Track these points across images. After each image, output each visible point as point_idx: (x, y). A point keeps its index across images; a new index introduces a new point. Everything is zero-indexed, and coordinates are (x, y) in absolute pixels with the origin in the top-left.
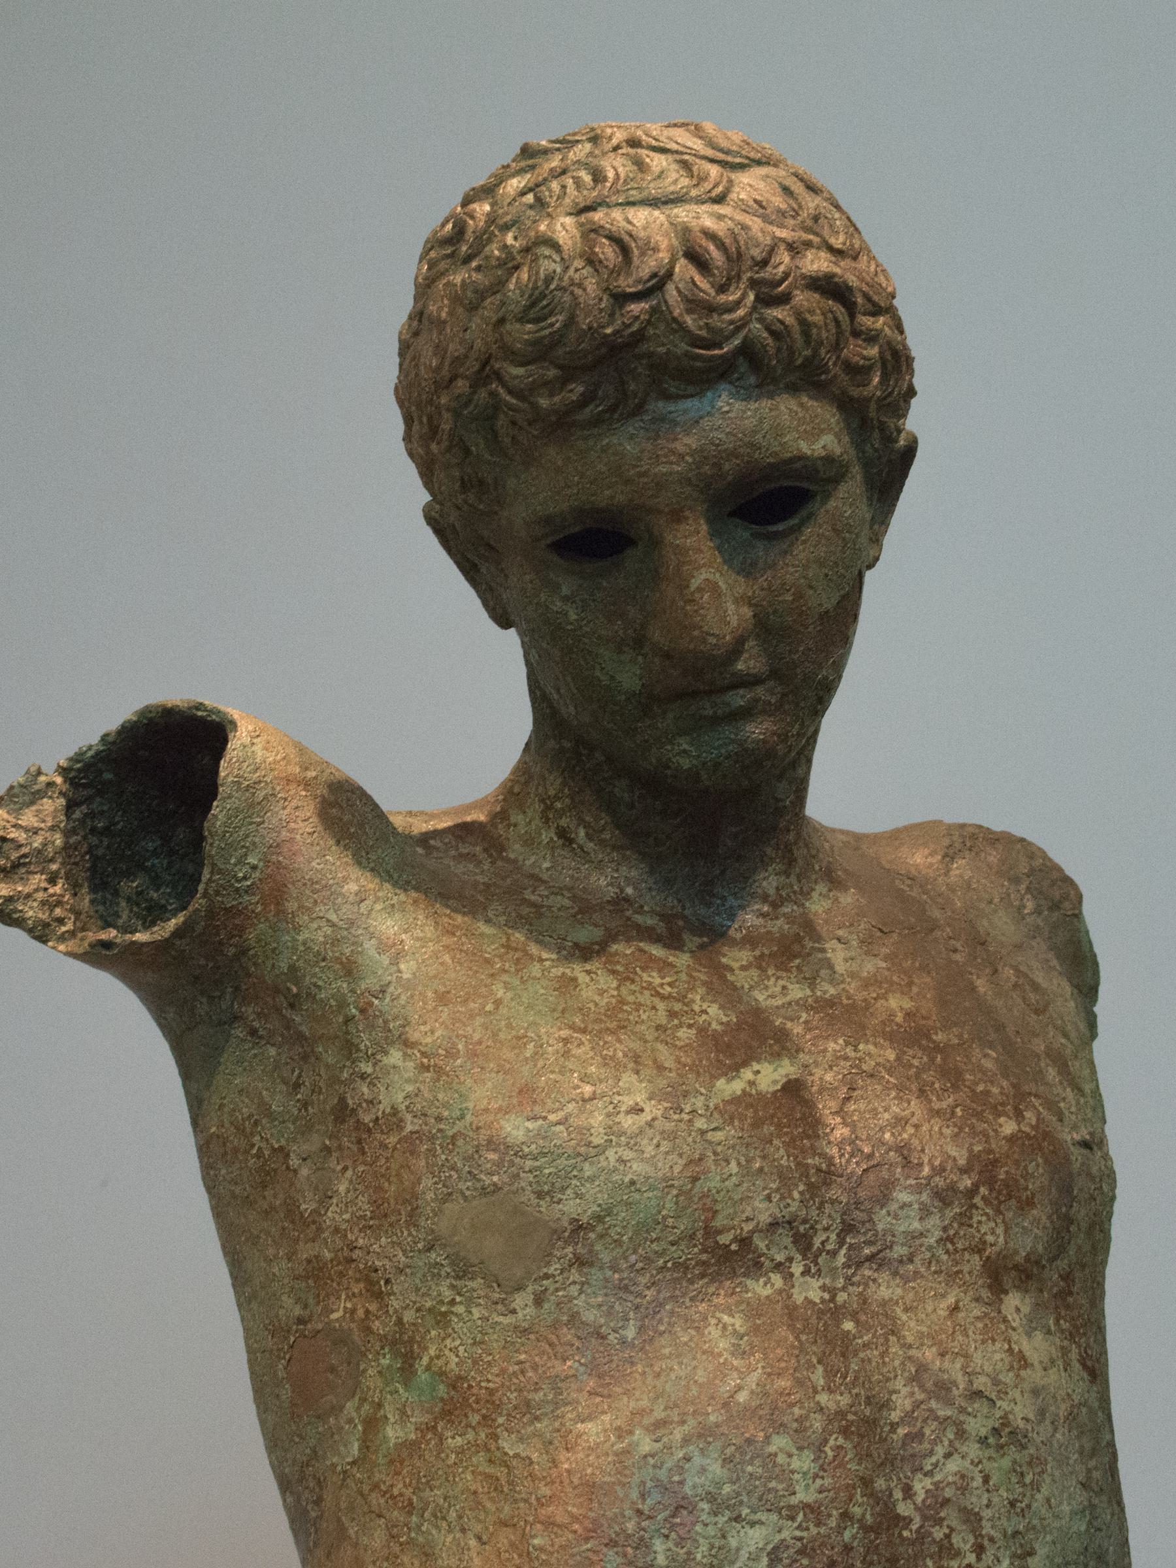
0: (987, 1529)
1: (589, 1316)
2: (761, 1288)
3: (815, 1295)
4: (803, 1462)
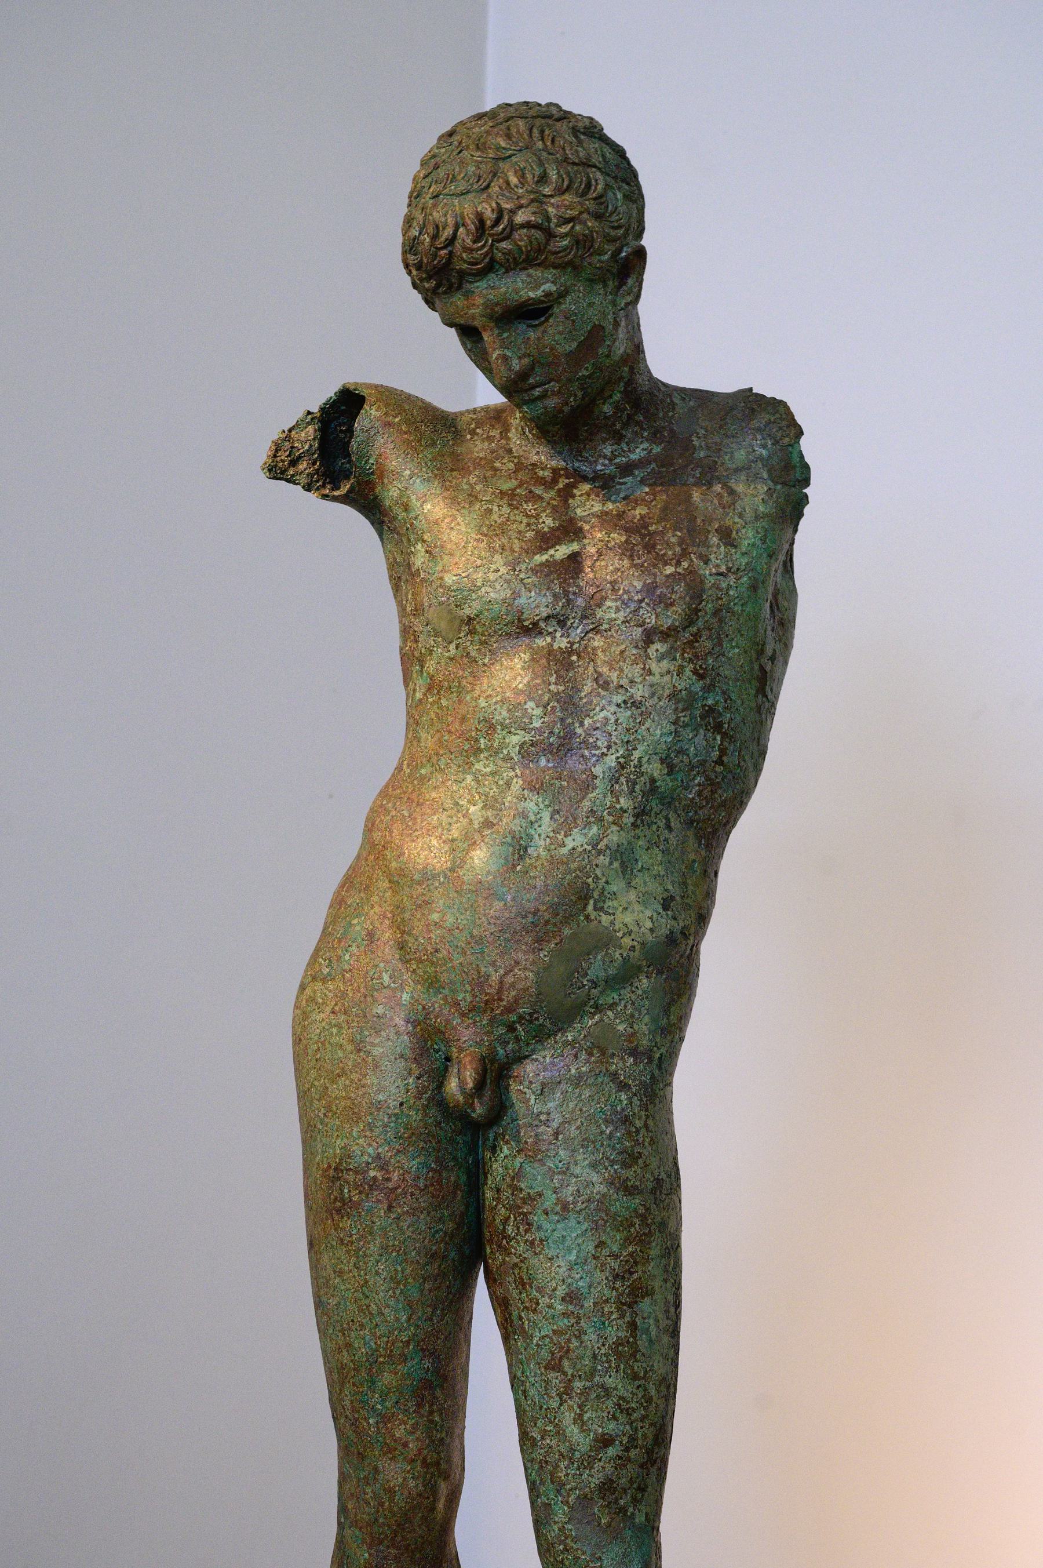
0: (614, 739)
1: (473, 654)
2: (540, 642)
3: (563, 646)
4: (538, 712)
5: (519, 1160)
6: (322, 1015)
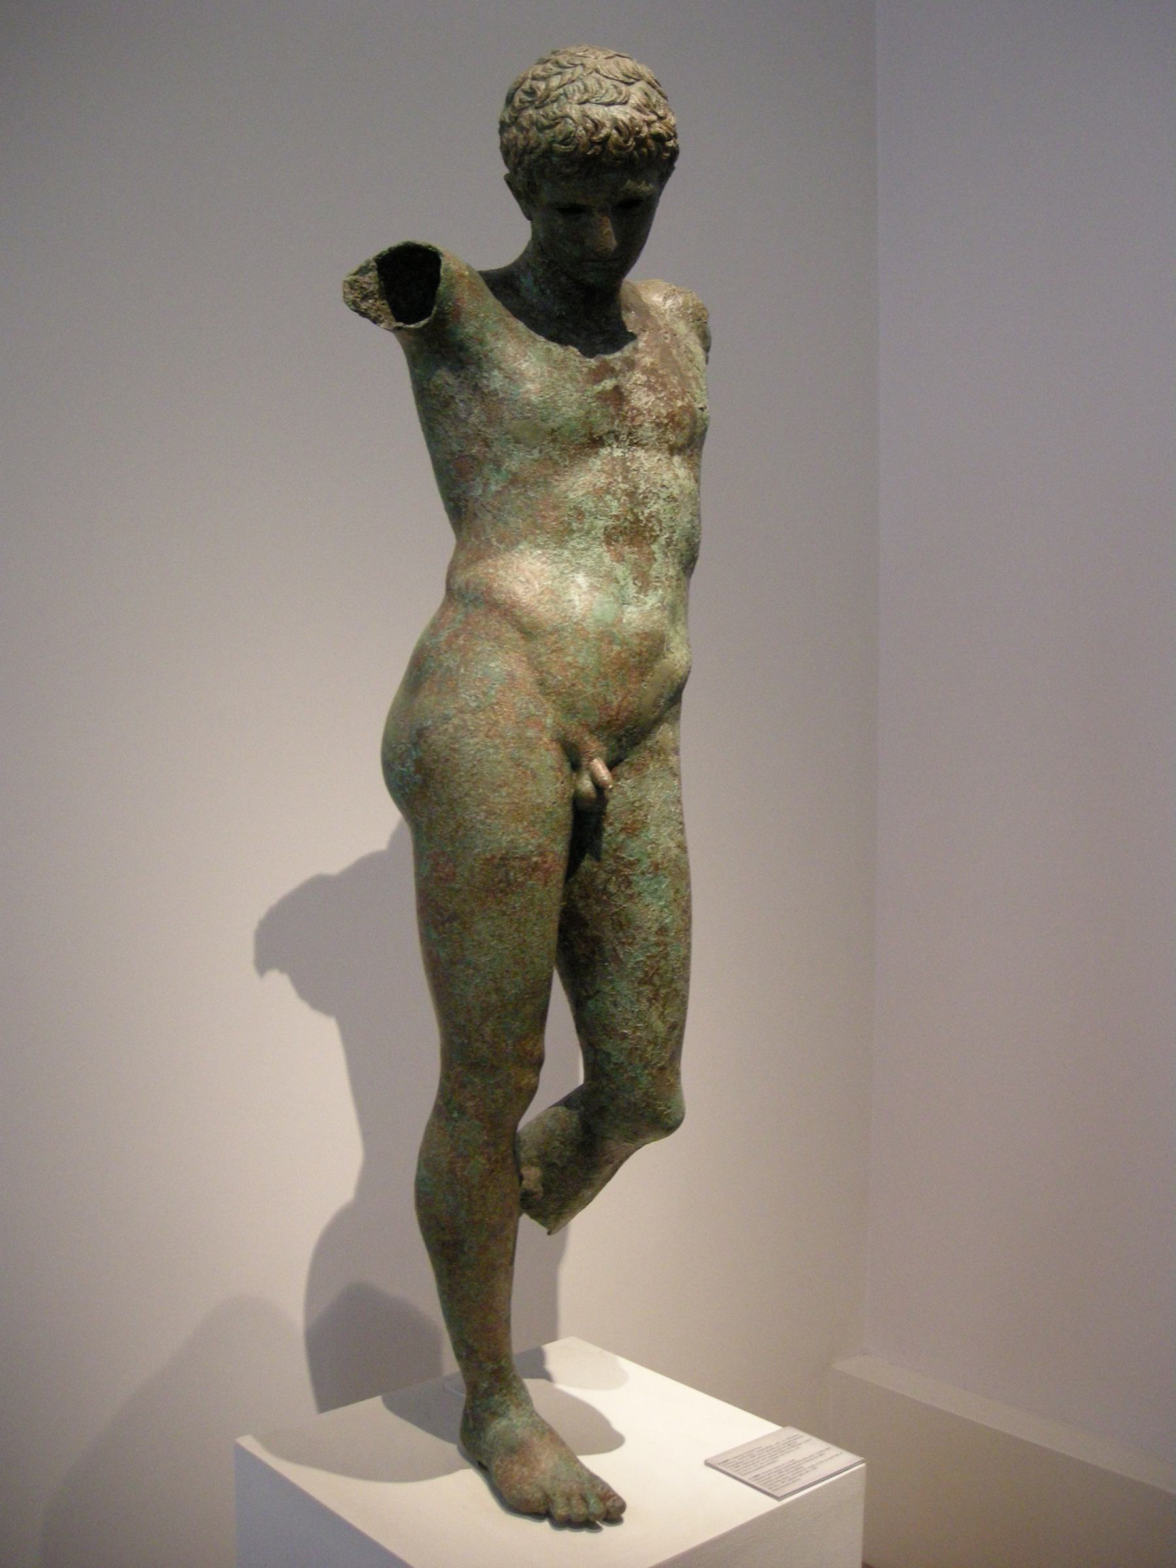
1: (556, 457)
5: (622, 837)
6: (476, 740)
